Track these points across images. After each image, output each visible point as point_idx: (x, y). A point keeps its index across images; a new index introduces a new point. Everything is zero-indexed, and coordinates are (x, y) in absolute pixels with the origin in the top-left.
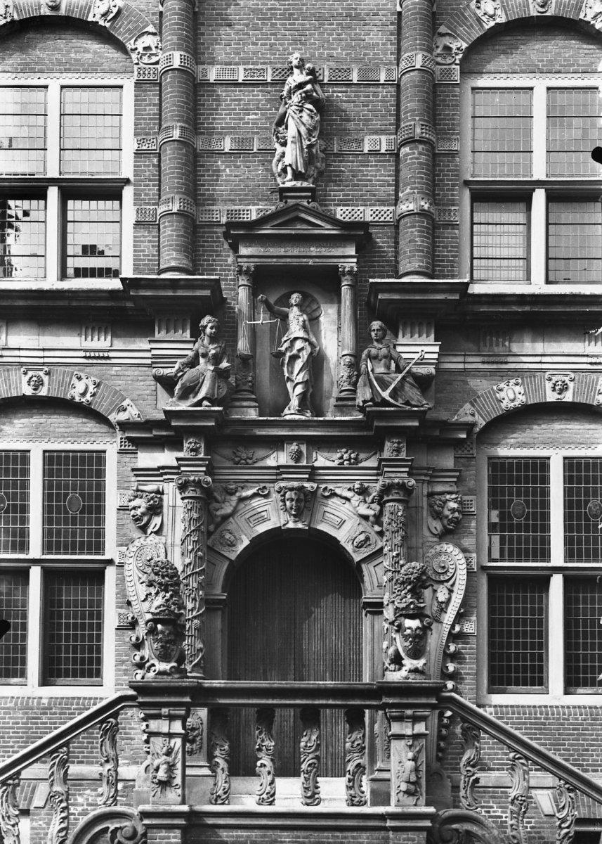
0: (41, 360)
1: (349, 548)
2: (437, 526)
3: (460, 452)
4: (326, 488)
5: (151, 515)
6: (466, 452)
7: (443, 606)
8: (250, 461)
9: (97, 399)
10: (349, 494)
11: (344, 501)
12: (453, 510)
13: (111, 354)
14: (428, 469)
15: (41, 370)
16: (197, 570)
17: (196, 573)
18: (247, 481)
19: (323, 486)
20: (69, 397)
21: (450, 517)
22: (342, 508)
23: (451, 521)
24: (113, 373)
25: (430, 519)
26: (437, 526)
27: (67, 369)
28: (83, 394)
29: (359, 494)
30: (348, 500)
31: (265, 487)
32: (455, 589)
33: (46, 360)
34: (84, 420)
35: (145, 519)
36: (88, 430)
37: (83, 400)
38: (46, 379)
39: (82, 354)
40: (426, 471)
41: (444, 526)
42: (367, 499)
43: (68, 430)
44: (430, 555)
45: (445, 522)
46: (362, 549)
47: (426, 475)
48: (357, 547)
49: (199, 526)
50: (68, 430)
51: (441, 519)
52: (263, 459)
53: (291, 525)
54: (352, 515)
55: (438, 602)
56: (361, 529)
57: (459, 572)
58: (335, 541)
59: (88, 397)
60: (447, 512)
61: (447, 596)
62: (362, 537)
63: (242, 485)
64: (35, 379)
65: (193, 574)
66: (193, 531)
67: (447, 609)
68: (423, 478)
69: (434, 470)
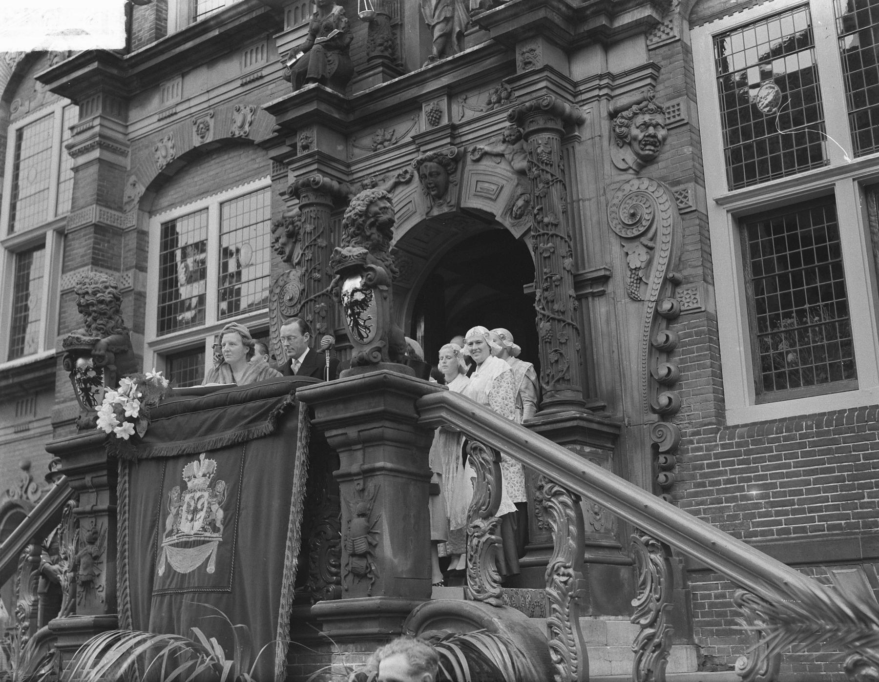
0: (205, 105)
1: (507, 223)
2: (628, 156)
3: (655, 40)
4: (475, 150)
5: (295, 243)
6: (664, 37)
7: (640, 274)
8: (386, 144)
9: (254, 126)
10: (500, 148)
11: (498, 159)
12: (646, 125)
13: (264, 73)
14: (600, 77)
15: (206, 115)
16: (312, 297)
17: (311, 300)
18: (388, 170)
19: (471, 149)
20: (230, 136)
21: (641, 136)
22: (498, 170)
23: (644, 143)
24: (269, 92)
25: (614, 150)
26: (628, 156)
27: (230, 104)
28: (242, 127)
29: (513, 143)
30: (502, 155)
31: (406, 172)
32: (658, 245)
33: (212, 102)
34: (254, 157)
35: (287, 250)
36: (257, 166)
37: (242, 133)
38: (212, 123)
39: (239, 83)
40: (597, 82)
41: (637, 154)
42: (525, 147)
43: (240, 172)
44: (616, 201)
45: (636, 145)
46: (524, 218)
47: (600, 88)
48: (515, 218)
49: (315, 240)
50: (240, 172)
51: (630, 144)
52: (403, 136)
53: (436, 212)
54: (510, 174)
55: (631, 270)
56: (519, 191)
57: (660, 216)
58: (488, 218)
59: (247, 128)
60: (635, 132)
61: (645, 257)
62: (520, 203)
63: (382, 176)
64: (201, 126)
65: (307, 302)
66: (307, 247)
67: (648, 278)
68: (596, 92)
69: (613, 77)
